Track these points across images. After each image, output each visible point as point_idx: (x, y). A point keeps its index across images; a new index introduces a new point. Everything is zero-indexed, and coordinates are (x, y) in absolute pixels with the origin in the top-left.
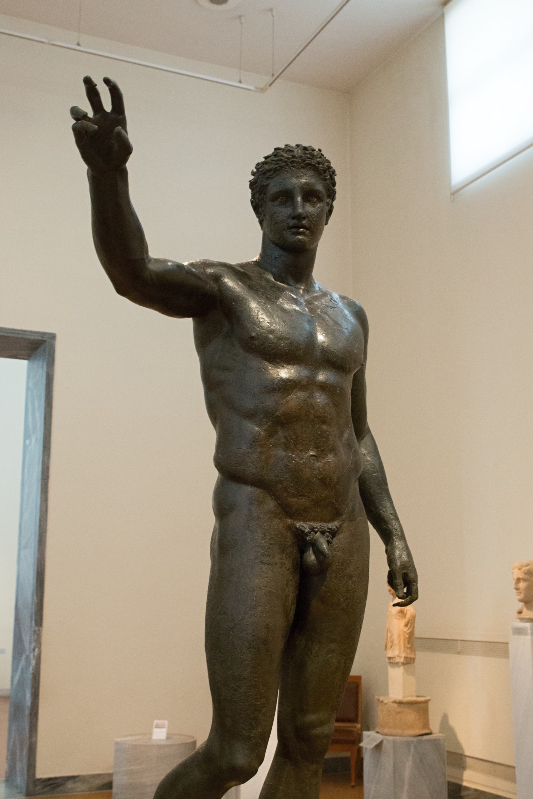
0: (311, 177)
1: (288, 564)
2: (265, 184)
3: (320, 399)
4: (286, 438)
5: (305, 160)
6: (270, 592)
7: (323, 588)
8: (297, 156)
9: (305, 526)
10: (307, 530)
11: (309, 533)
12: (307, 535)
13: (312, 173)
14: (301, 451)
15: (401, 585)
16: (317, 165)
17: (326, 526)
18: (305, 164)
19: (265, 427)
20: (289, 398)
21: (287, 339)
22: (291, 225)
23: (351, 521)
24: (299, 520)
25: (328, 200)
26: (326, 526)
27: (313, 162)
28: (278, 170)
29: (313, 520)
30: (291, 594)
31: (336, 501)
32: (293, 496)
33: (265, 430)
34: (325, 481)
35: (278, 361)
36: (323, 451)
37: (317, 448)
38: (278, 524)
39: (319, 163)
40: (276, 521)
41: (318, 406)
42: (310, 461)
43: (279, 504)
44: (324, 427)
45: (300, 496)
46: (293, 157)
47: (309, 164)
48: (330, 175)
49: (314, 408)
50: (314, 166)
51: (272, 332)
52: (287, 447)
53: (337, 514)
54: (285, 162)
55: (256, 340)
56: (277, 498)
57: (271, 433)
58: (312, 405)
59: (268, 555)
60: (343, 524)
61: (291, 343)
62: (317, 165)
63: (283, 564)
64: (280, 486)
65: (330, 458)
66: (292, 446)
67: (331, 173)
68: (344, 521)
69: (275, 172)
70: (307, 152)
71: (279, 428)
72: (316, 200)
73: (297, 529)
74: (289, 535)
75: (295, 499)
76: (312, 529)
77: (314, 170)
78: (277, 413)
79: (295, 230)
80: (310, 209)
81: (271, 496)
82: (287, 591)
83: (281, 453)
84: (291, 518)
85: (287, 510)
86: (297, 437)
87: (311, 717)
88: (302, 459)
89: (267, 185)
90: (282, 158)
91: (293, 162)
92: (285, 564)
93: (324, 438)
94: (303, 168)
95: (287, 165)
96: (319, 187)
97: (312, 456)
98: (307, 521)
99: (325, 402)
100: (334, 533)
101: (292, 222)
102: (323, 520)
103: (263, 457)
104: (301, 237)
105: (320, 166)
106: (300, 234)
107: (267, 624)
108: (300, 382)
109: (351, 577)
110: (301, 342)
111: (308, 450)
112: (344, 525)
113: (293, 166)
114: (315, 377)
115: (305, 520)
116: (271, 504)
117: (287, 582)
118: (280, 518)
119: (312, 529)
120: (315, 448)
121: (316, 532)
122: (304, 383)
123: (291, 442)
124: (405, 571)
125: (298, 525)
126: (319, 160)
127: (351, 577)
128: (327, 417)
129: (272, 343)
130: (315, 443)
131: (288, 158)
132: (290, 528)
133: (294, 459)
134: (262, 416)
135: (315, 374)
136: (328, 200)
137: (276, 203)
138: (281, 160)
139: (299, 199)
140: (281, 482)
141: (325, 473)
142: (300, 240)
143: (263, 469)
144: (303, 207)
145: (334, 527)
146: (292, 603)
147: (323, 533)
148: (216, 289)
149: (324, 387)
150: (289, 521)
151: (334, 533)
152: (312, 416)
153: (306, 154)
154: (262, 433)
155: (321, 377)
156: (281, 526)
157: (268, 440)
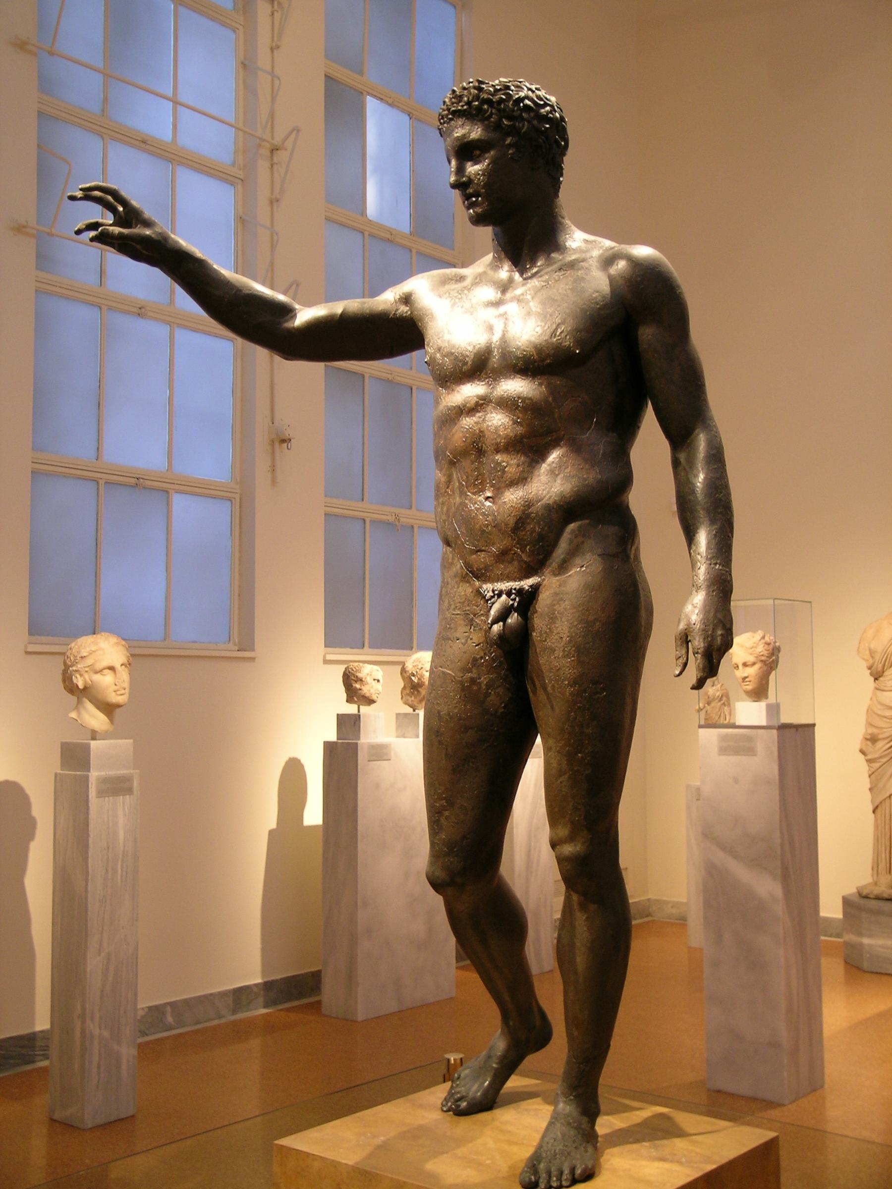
23: (555, 575)
25: (508, 141)
29: (499, 579)
31: (523, 552)
38: (465, 590)
39: (469, 103)
44: (499, 457)
58: (481, 432)
60: (544, 580)
65: (513, 497)
72: (478, 152)
82: (474, 671)
88: (476, 503)
94: (451, 119)
96: (476, 133)
99: (500, 423)
102: (509, 578)
108: (464, 406)
109: (553, 650)
110: (468, 353)
121: (499, 595)
127: (553, 650)
136: (508, 141)
146: (488, 686)
147: (509, 594)
150: (477, 583)
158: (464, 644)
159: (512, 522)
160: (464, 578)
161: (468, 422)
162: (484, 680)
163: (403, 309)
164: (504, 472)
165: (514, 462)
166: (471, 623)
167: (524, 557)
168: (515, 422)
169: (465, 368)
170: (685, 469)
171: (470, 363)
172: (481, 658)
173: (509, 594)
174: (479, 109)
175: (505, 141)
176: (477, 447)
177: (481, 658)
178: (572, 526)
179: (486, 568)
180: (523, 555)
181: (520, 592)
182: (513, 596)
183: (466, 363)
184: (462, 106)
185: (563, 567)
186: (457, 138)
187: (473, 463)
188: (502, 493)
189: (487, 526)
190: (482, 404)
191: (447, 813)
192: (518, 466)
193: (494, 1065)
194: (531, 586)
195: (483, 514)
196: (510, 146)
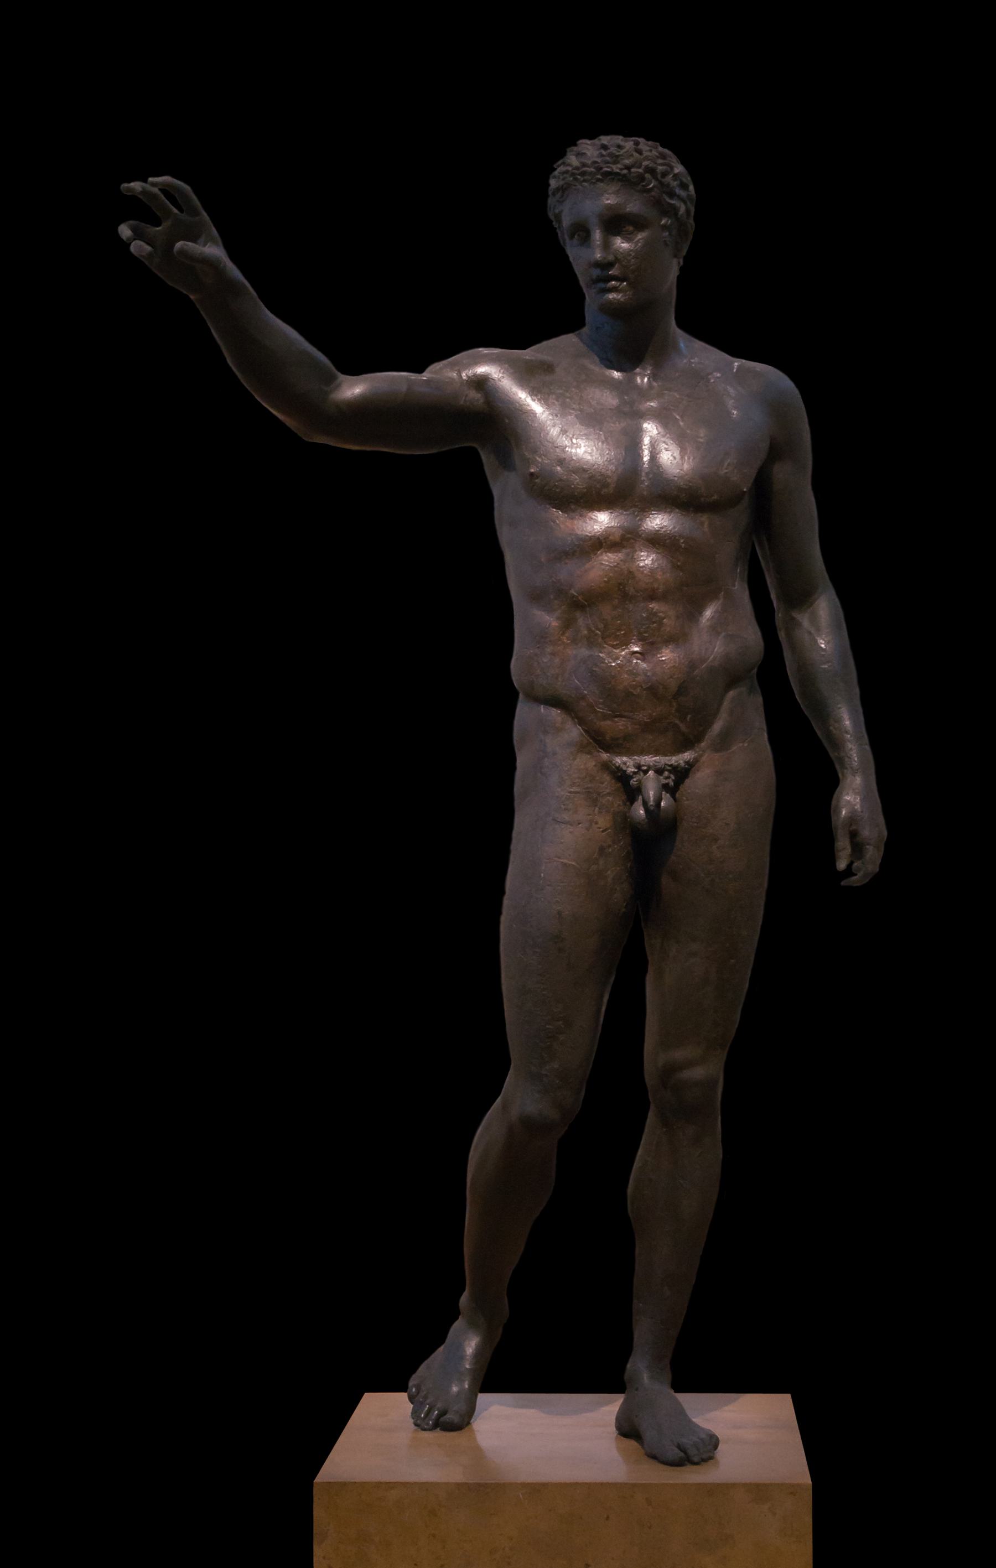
0: (617, 193)
1: (604, 821)
2: (557, 211)
3: (647, 559)
4: (589, 630)
5: (601, 168)
6: (565, 864)
7: (673, 857)
8: (589, 162)
9: (627, 762)
10: (631, 770)
11: (635, 773)
12: (632, 777)
13: (613, 187)
14: (615, 647)
15: (844, 849)
16: (625, 171)
17: (661, 760)
18: (602, 175)
19: (558, 613)
20: (587, 566)
21: (585, 470)
22: (594, 277)
23: (717, 751)
24: (620, 754)
25: (663, 222)
26: (661, 760)
27: (616, 168)
28: (566, 189)
29: (642, 752)
30: (614, 870)
32: (605, 717)
33: (558, 618)
34: (654, 691)
35: (573, 507)
36: (652, 643)
37: (641, 639)
38: (586, 762)
39: (628, 168)
40: (585, 757)
41: (642, 572)
42: (630, 662)
43: (586, 731)
44: (654, 606)
45: (616, 717)
46: (584, 165)
47: (610, 173)
48: (657, 179)
49: (634, 577)
50: (617, 174)
51: (561, 462)
52: (591, 642)
53: (686, 743)
54: (573, 174)
55: (537, 477)
56: (581, 721)
57: (568, 624)
58: (630, 572)
59: (565, 809)
60: (701, 756)
61: (590, 478)
62: (625, 171)
63: (592, 822)
64: (583, 704)
65: (666, 655)
66: (600, 640)
67: (659, 176)
68: (704, 751)
69: (563, 192)
70: (604, 153)
71: (578, 614)
72: (631, 228)
73: (619, 769)
74: (607, 778)
75: (609, 722)
76: (639, 767)
77: (619, 180)
78: (573, 592)
79: (602, 285)
80: (621, 244)
81: (573, 719)
82: (601, 862)
83: (584, 652)
84: (607, 751)
85: (598, 740)
86: (606, 626)
87: (679, 1055)
88: (617, 658)
89: (561, 212)
90: (570, 169)
91: (583, 174)
92: (596, 823)
93: (654, 623)
94: (598, 180)
95: (576, 179)
96: (634, 206)
97: (636, 652)
98: (633, 754)
99: (656, 565)
100: (682, 774)
101: (596, 272)
102: (657, 753)
103: (557, 660)
104: (611, 296)
105: (633, 170)
106: (614, 289)
107: (559, 913)
108: (606, 538)
110: (609, 472)
111: (625, 643)
112: (704, 758)
113: (584, 181)
114: (640, 526)
115: (629, 753)
116: (574, 732)
117: (602, 849)
118: (589, 753)
119: (639, 767)
120: (640, 640)
121: (646, 772)
122: (617, 537)
123: (596, 635)
124: (854, 827)
125: (618, 760)
126: (627, 162)
128: (658, 588)
129: (561, 480)
130: (640, 633)
131: (577, 168)
132: (606, 766)
133: (602, 661)
134: (552, 597)
135: (640, 520)
136: (663, 222)
137: (575, 241)
138: (567, 172)
139: (597, 235)
140: (583, 697)
141: (654, 678)
142: (611, 302)
143: (557, 678)
144: (606, 246)
145: (682, 764)
147: (659, 772)
148: (482, 401)
149: (656, 541)
150: (605, 756)
151: (682, 774)
152: (632, 591)
153: (602, 156)
154: (555, 624)
155: (657, 521)
156: (591, 764)
157: (563, 634)
158: (588, 829)
159: (673, 686)
160: (582, 748)
161: (608, 559)
162: (610, 874)
163: (475, 396)
164: (660, 623)
165: (672, 613)
166: (594, 802)
167: (683, 727)
168: (675, 567)
169: (604, 491)
170: (810, 633)
171: (613, 486)
172: (609, 846)
173: (659, 772)
174: (641, 178)
175: (661, 220)
176: (623, 589)
177: (609, 846)
178: (731, 693)
179: (627, 737)
180: (681, 725)
181: (674, 769)
182: (666, 773)
183: (606, 485)
184: (621, 169)
185: (723, 743)
186: (609, 207)
187: (615, 608)
188: (658, 650)
189: (635, 687)
190: (629, 539)
191: (562, 1037)
192: (678, 617)
193: (468, 1366)
194: (687, 763)
195: (630, 672)
196: (664, 227)
